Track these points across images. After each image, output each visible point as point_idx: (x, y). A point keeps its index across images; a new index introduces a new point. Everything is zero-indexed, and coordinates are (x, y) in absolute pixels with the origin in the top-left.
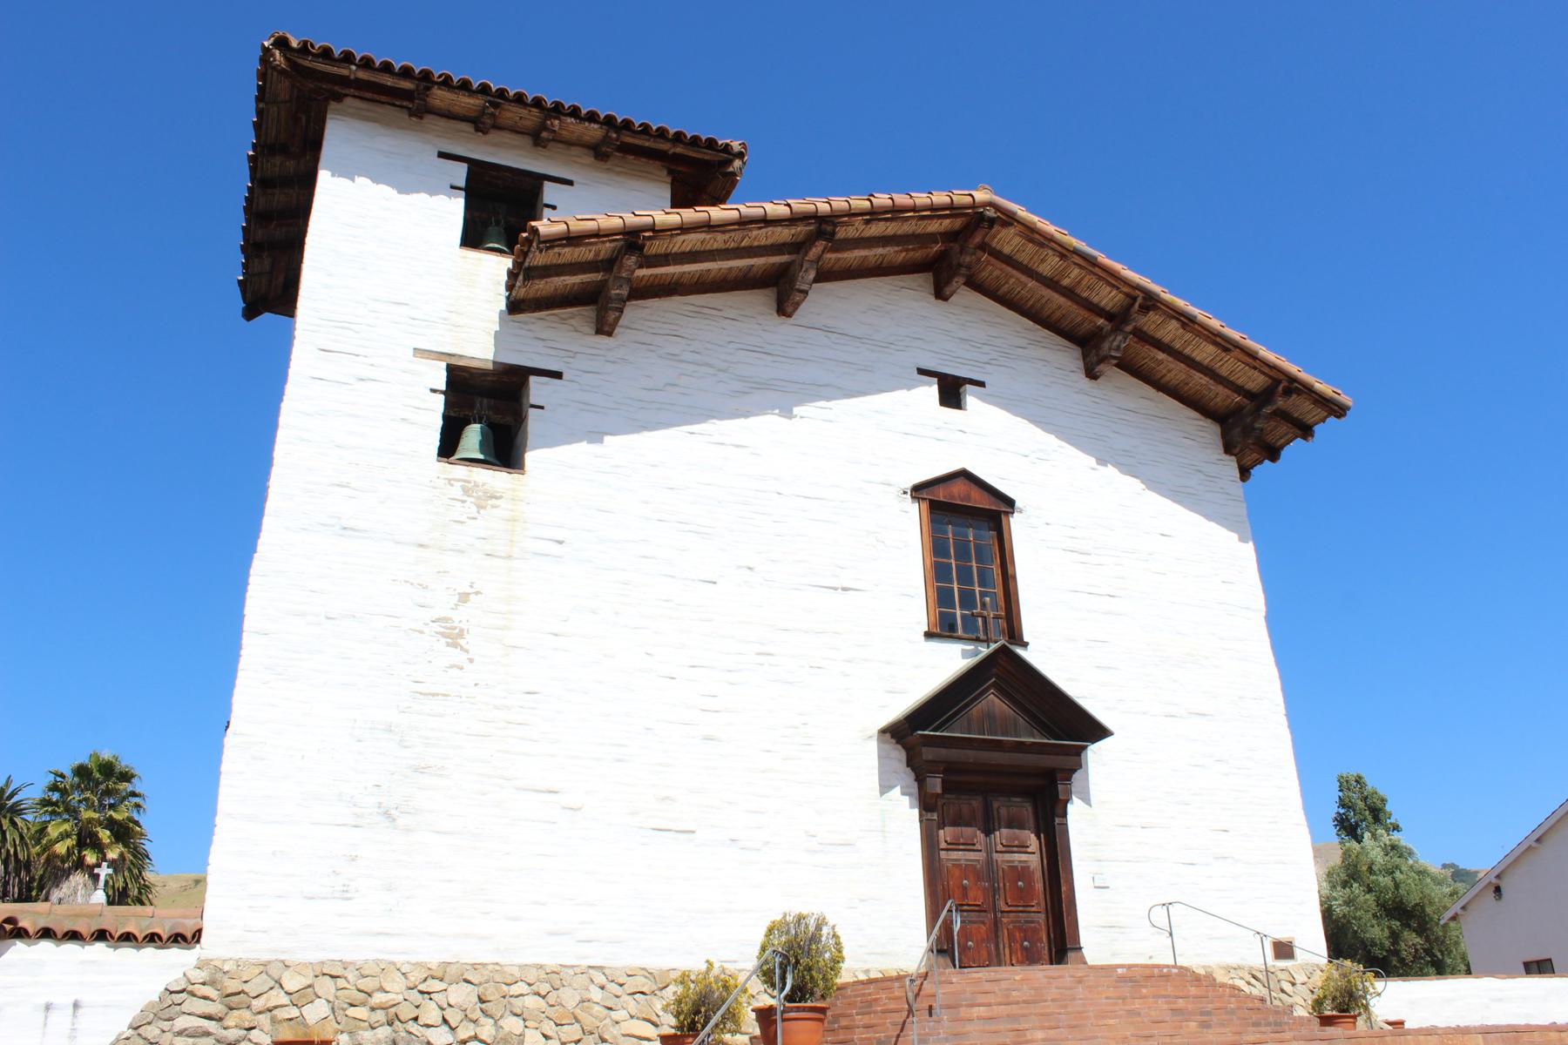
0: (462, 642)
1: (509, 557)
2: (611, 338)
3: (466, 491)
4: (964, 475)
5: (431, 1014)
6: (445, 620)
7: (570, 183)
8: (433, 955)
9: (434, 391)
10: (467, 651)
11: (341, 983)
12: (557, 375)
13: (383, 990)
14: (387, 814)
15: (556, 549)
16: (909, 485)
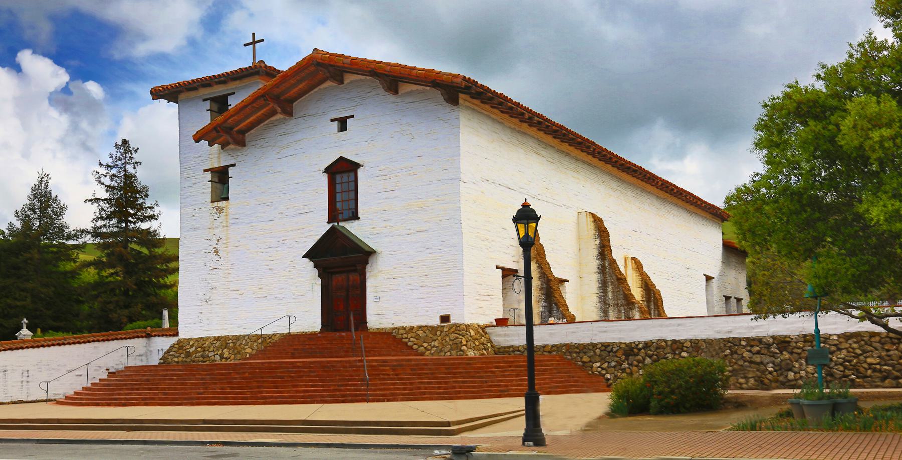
0: (218, 253)
1: (227, 226)
2: (245, 148)
3: (217, 210)
4: (341, 158)
5: (211, 349)
6: (215, 248)
7: (234, 93)
8: (216, 335)
9: (209, 181)
10: (219, 256)
11: (199, 343)
12: (234, 165)
13: (205, 344)
14: (206, 301)
15: (237, 221)
16: (323, 169)
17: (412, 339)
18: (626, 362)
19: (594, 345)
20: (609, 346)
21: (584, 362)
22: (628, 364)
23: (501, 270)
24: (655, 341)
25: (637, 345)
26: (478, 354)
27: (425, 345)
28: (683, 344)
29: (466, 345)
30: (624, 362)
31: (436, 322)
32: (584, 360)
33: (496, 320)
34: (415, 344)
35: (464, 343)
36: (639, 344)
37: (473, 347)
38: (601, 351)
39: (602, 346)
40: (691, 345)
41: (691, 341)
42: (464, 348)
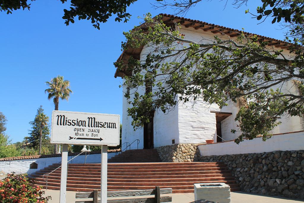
17: (162, 153)
18: (253, 168)
19: (241, 155)
20: (248, 156)
21: (233, 168)
22: (254, 170)
23: (215, 113)
24: (274, 152)
25: (262, 156)
26: (181, 161)
27: (164, 156)
28: (291, 154)
29: (175, 156)
30: (252, 168)
31: (171, 144)
32: (233, 166)
33: (207, 141)
34: (161, 156)
35: (174, 155)
36: (264, 154)
37: (180, 157)
38: (243, 160)
39: (245, 156)
40: (297, 155)
41: (297, 152)
42: (174, 158)
